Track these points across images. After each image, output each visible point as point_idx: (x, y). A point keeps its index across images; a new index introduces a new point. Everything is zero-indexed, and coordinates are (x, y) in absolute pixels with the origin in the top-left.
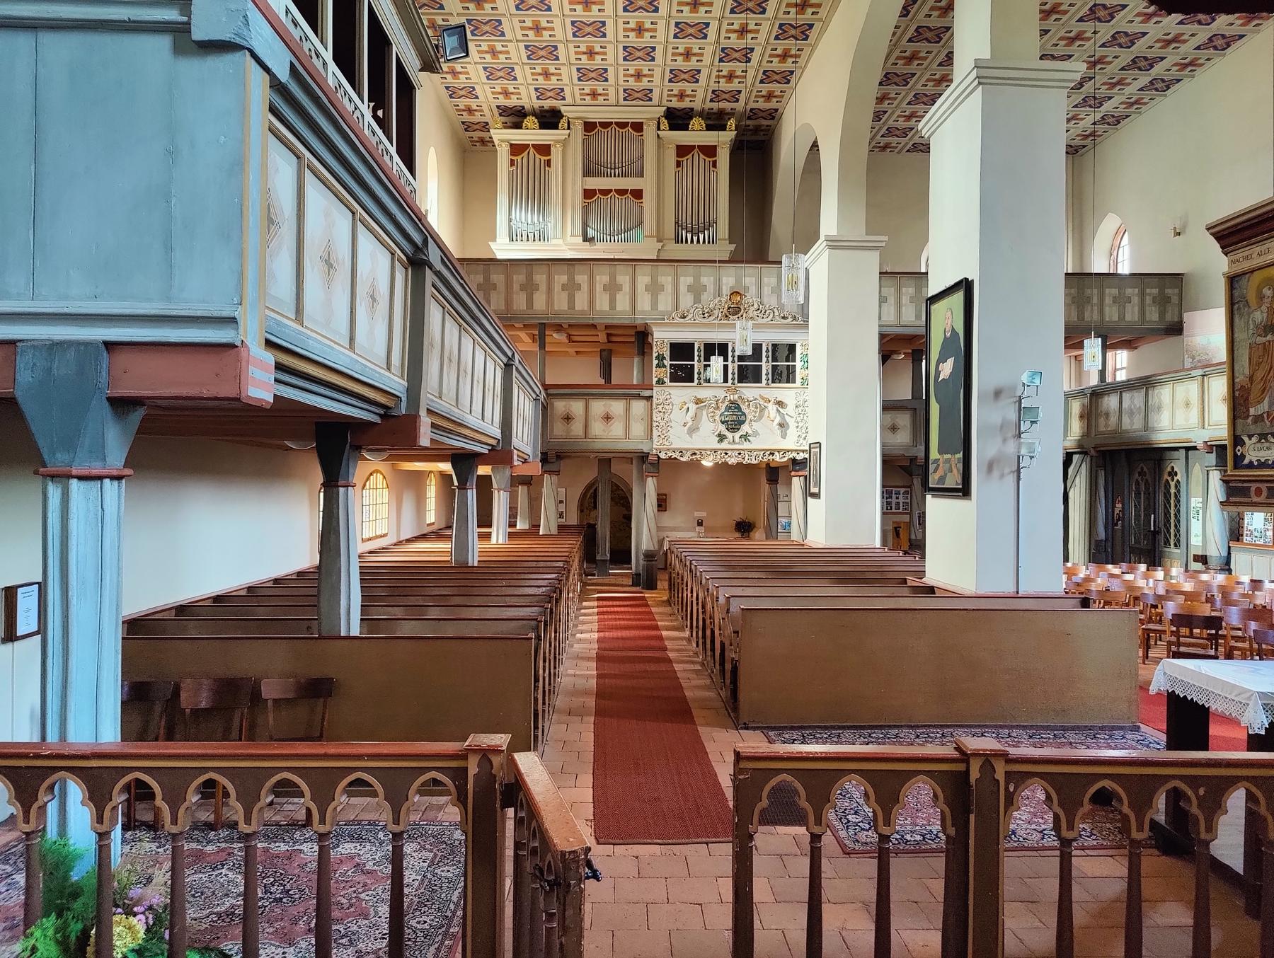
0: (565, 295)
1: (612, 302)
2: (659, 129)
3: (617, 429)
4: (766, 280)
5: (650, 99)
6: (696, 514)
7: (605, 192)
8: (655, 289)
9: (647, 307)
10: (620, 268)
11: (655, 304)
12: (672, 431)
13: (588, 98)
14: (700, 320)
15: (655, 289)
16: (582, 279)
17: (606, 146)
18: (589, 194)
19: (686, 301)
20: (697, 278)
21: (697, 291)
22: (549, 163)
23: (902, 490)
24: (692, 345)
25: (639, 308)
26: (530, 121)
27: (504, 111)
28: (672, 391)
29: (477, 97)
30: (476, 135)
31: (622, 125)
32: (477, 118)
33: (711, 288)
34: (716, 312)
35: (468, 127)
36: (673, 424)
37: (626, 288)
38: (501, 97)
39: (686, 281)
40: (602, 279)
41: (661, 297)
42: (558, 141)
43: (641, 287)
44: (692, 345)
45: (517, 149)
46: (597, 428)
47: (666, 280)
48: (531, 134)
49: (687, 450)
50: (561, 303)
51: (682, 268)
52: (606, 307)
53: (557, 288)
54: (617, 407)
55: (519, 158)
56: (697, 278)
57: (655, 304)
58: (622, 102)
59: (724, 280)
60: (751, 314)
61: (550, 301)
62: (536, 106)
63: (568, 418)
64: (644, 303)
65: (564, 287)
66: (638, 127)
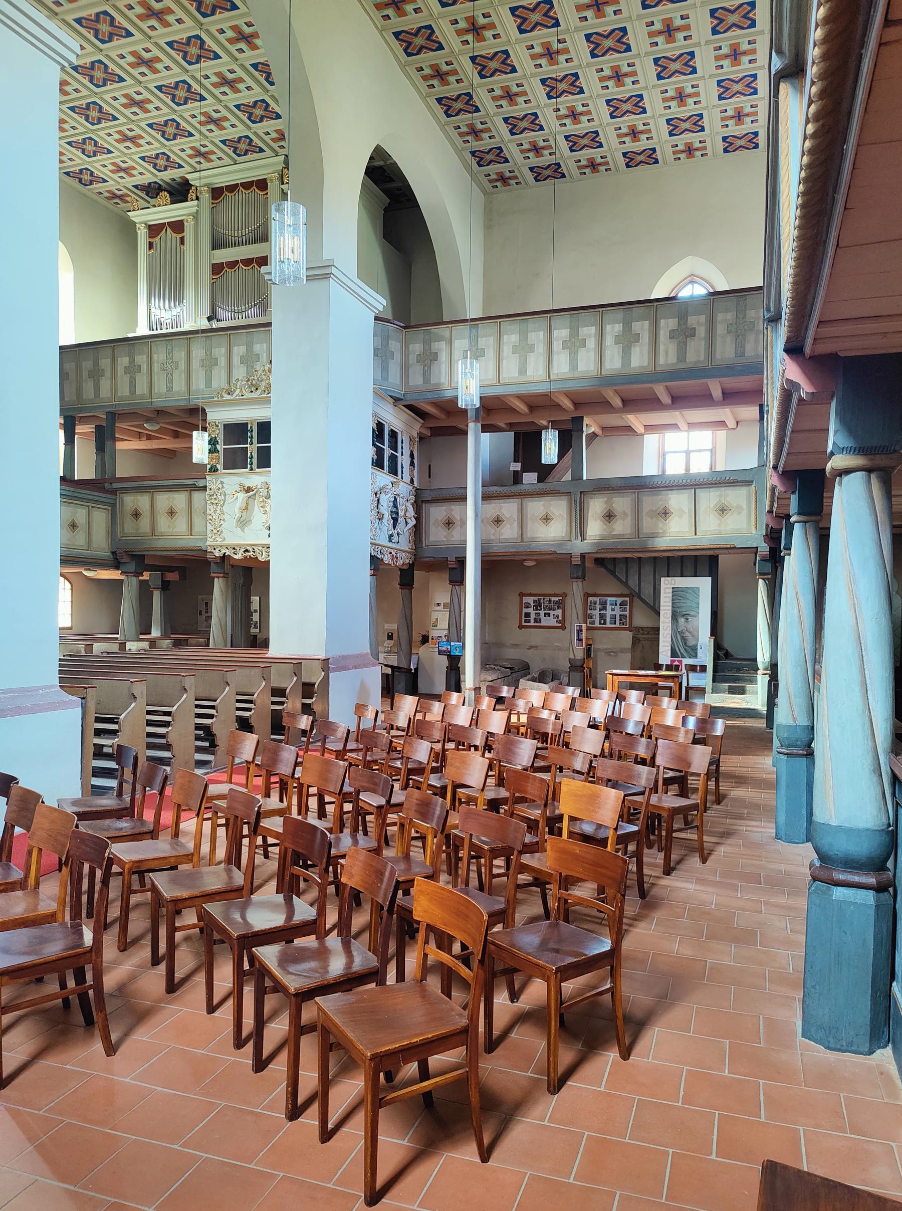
0: (127, 378)
1: (170, 381)
3: (180, 525)
6: (387, 626)
7: (233, 264)
8: (210, 363)
9: (202, 385)
12: (225, 525)
16: (141, 359)
18: (217, 269)
22: (182, 240)
23: (619, 600)
25: (193, 387)
28: (225, 480)
31: (247, 185)
36: (226, 517)
40: (160, 356)
41: (215, 372)
42: (188, 215)
45: (154, 230)
46: (163, 524)
49: (240, 546)
52: (164, 390)
53: (120, 371)
54: (179, 500)
55: (157, 239)
61: (114, 389)
63: (136, 515)
64: (199, 383)
65: (127, 370)
66: (262, 184)
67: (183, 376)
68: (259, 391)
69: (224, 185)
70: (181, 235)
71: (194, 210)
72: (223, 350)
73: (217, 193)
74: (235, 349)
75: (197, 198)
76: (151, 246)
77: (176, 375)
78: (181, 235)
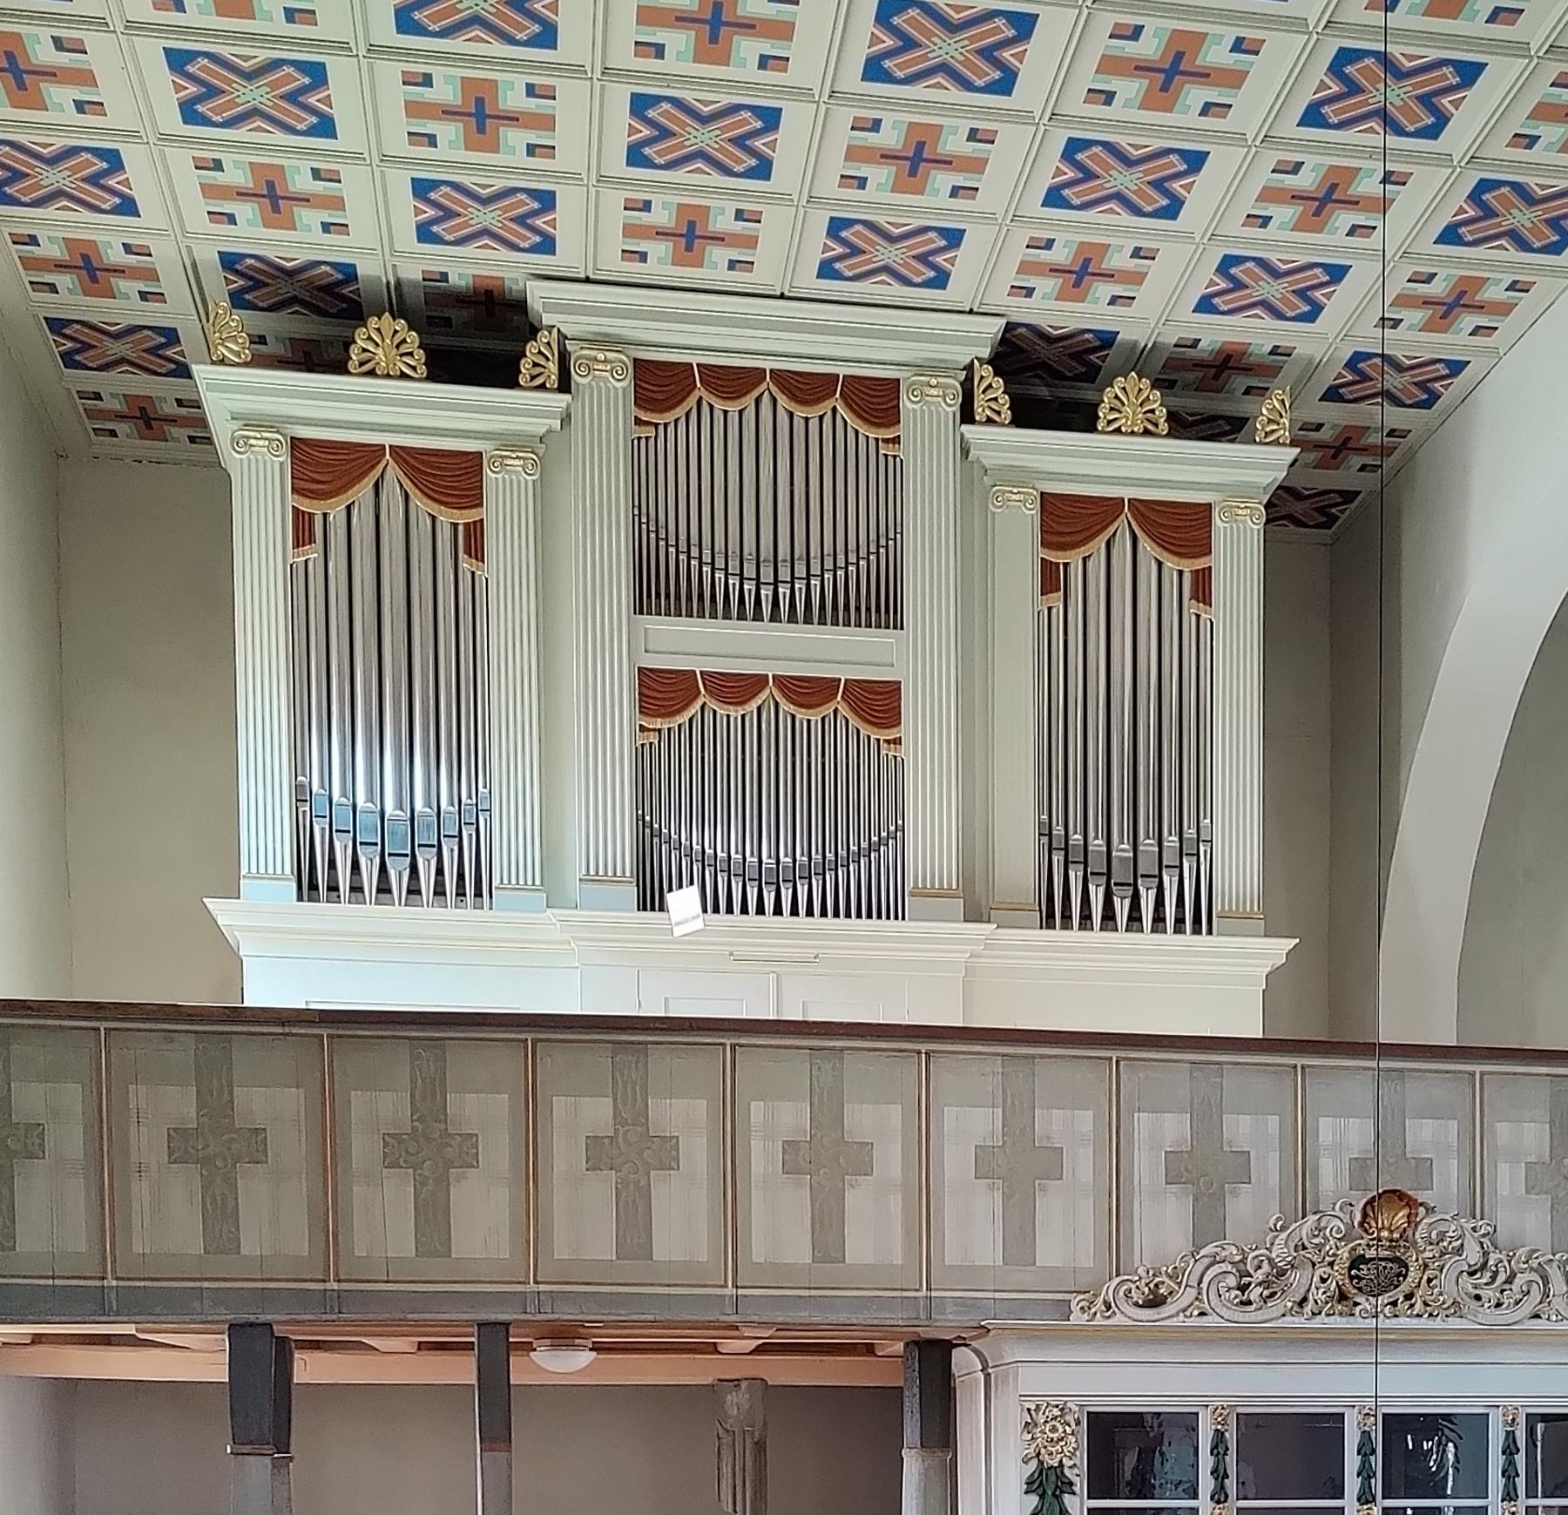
2: (967, 415)
4: (1503, 1132)
5: (941, 280)
8: (1020, 1169)
10: (863, 1066)
11: (1020, 1236)
13: (658, 250)
14: (1224, 1314)
15: (1020, 1169)
17: (748, 472)
19: (1162, 1227)
20: (1207, 1118)
21: (1205, 1176)
24: (1188, 1423)
26: (382, 338)
27: (254, 283)
29: (128, 207)
30: (118, 385)
32: (123, 307)
33: (1269, 1168)
34: (1298, 1280)
35: (77, 344)
37: (891, 1160)
38: (246, 211)
39: (1159, 1131)
41: (1050, 1206)
42: (513, 443)
43: (955, 1162)
44: (1188, 1423)
45: (322, 467)
47: (1071, 1126)
48: (389, 402)
50: (583, 1229)
51: (1140, 1074)
52: (798, 1249)
55: (336, 510)
56: (1207, 1118)
57: (1020, 1236)
58: (809, 282)
59: (1326, 1129)
60: (1451, 1283)
62: (412, 272)
67: (895, 1203)
68: (1276, 1307)
69: (694, 359)
70: (470, 516)
71: (539, 426)
72: (1086, 1120)
73: (659, 384)
74: (1143, 1123)
75: (565, 386)
76: (303, 530)
77: (858, 1200)
78: (470, 516)
